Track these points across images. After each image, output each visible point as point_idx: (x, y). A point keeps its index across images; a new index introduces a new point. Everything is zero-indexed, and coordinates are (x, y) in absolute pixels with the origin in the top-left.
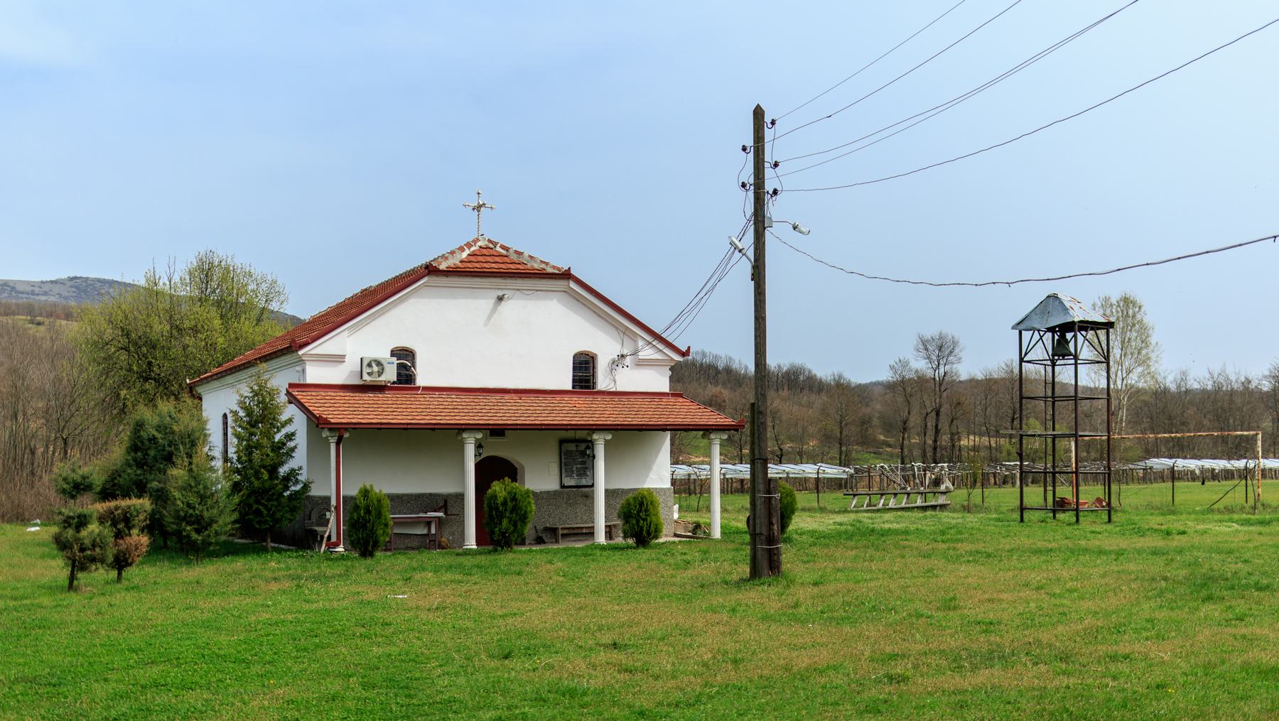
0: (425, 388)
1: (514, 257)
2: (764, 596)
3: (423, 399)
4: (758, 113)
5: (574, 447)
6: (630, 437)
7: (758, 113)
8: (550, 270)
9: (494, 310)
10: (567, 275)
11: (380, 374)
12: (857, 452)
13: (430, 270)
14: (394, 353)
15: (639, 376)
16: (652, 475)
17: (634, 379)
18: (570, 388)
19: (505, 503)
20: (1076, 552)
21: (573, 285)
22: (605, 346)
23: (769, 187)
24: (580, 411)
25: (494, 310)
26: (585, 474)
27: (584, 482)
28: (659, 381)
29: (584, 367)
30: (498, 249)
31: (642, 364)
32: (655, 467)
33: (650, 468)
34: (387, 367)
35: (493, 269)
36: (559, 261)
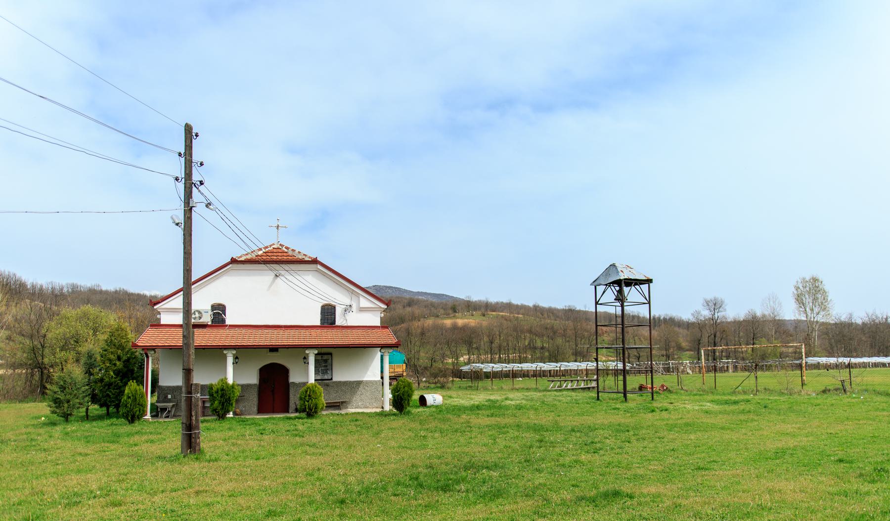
0: (231, 326)
1: (290, 253)
2: (191, 467)
3: (227, 331)
4: (188, 129)
5: (326, 357)
6: (357, 350)
7: (188, 129)
8: (307, 259)
9: (274, 281)
10: (315, 261)
11: (200, 318)
12: (469, 362)
13: (234, 261)
14: (214, 307)
15: (362, 315)
16: (369, 373)
17: (355, 319)
18: (318, 323)
19: (217, 392)
20: (302, 445)
21: (319, 267)
22: (338, 297)
23: (196, 178)
24: (329, 337)
25: (274, 281)
26: (327, 373)
27: (326, 377)
28: (374, 320)
29: (328, 313)
30: (284, 248)
31: (362, 310)
32: (371, 368)
33: (368, 369)
34: (204, 314)
35: (276, 260)
36: (312, 254)
